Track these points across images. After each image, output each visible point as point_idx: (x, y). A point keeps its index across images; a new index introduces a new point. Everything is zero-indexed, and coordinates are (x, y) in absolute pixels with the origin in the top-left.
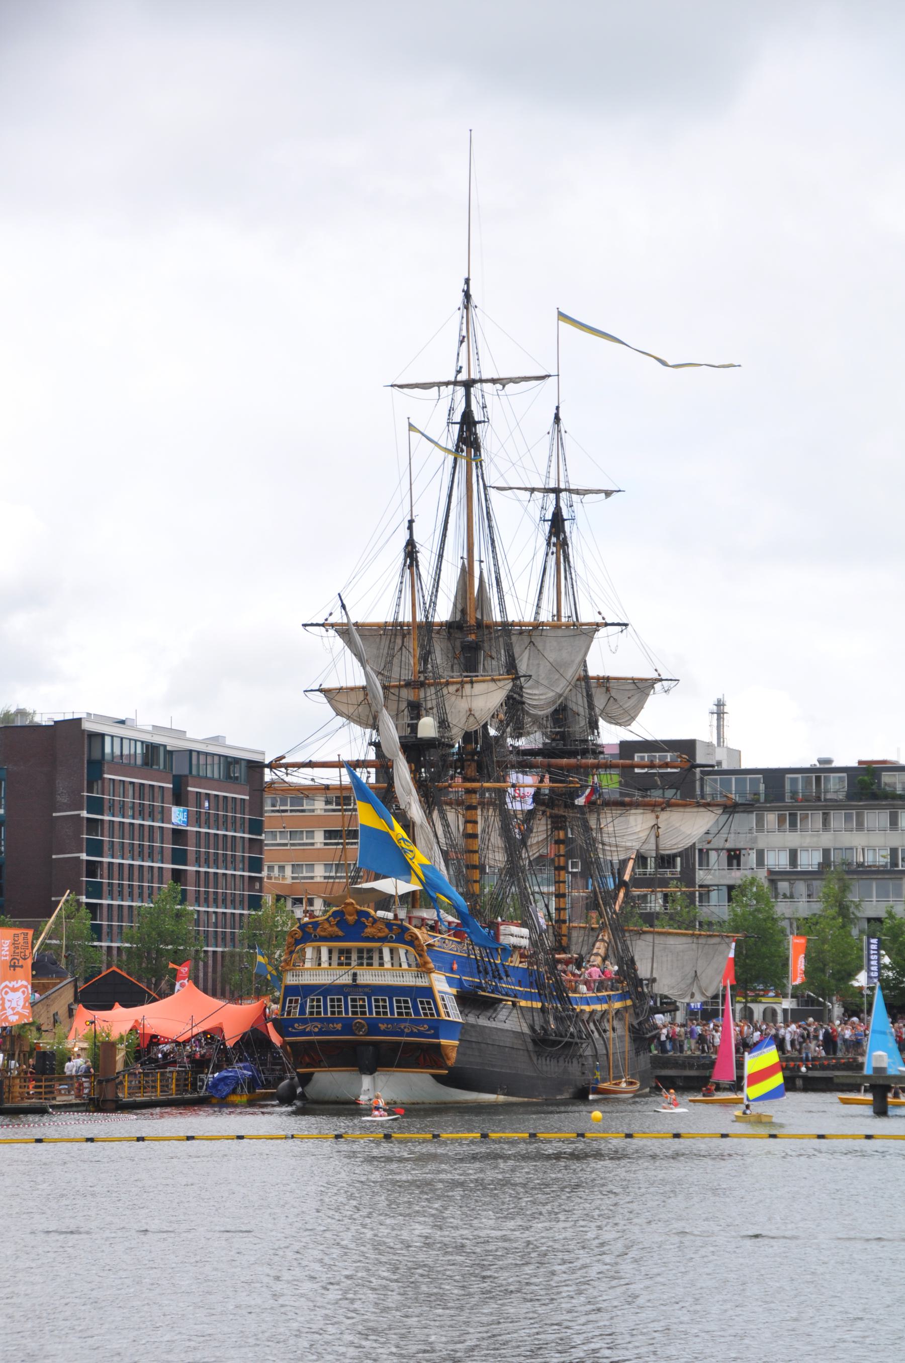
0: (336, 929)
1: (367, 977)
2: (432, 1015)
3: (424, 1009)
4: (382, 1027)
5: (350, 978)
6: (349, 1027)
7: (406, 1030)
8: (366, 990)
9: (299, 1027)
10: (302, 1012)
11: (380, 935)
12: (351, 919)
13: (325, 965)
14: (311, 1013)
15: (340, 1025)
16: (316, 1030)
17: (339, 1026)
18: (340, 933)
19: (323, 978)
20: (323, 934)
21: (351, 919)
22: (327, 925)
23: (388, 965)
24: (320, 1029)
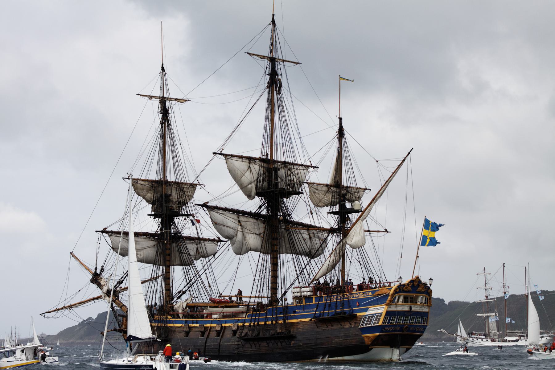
0: (410, 288)
1: (414, 309)
2: (425, 323)
3: (423, 321)
4: (411, 328)
5: (409, 308)
6: (402, 328)
7: (417, 330)
8: (411, 313)
9: (386, 328)
10: (388, 323)
11: (423, 291)
12: (416, 284)
13: (400, 303)
14: (391, 323)
15: (400, 328)
16: (391, 330)
17: (398, 328)
18: (411, 290)
19: (399, 308)
20: (406, 290)
21: (416, 284)
22: (408, 286)
23: (419, 303)
24: (392, 330)
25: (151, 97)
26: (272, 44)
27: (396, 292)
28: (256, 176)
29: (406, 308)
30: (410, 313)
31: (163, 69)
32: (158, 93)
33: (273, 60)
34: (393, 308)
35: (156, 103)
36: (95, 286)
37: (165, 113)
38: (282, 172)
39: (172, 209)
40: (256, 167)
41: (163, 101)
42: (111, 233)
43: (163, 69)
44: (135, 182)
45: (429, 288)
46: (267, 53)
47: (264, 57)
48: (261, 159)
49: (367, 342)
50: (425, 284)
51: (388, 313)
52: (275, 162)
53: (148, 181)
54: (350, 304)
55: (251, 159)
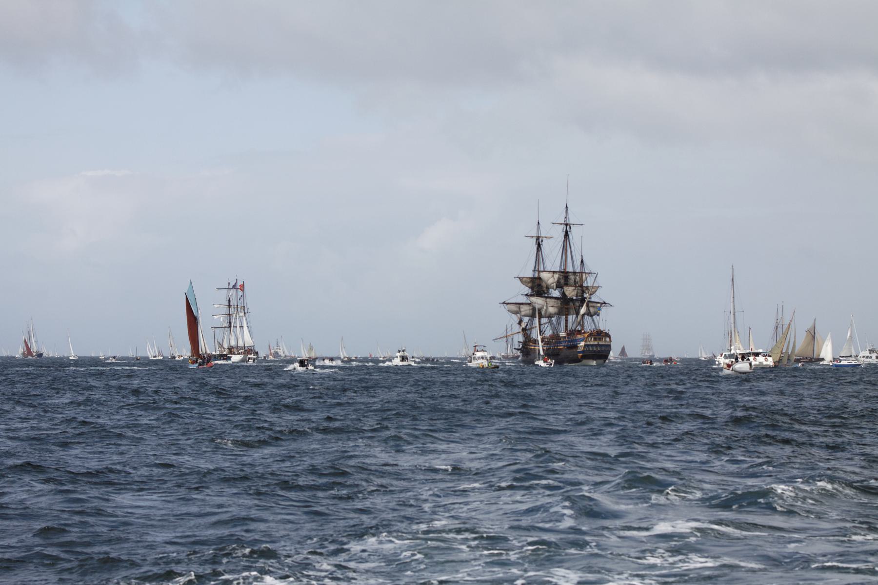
1: (600, 343)
6: (595, 352)
19: (592, 343)
25: (532, 237)
26: (566, 218)
27: (588, 336)
28: (556, 280)
29: (596, 343)
30: (598, 345)
31: (538, 223)
32: (535, 235)
33: (567, 225)
34: (588, 343)
35: (534, 240)
36: (518, 326)
37: (539, 246)
38: (572, 277)
39: (544, 291)
40: (556, 276)
41: (538, 238)
42: (508, 304)
43: (538, 223)
44: (521, 279)
45: (608, 334)
46: (563, 222)
47: (562, 224)
48: (559, 272)
49: (579, 357)
50: (606, 333)
51: (585, 345)
52: (568, 272)
53: (529, 278)
54: (576, 340)
55: (554, 272)
